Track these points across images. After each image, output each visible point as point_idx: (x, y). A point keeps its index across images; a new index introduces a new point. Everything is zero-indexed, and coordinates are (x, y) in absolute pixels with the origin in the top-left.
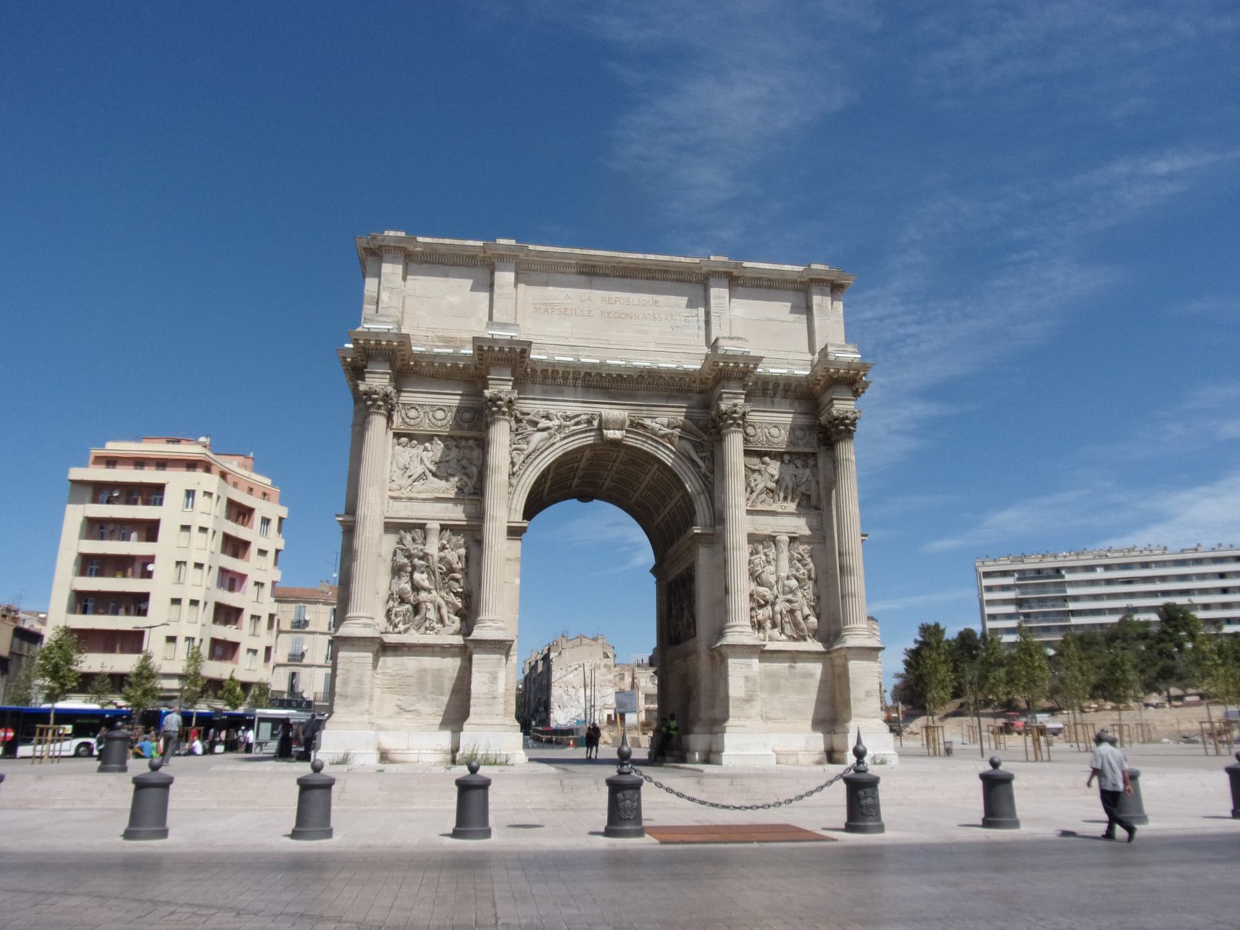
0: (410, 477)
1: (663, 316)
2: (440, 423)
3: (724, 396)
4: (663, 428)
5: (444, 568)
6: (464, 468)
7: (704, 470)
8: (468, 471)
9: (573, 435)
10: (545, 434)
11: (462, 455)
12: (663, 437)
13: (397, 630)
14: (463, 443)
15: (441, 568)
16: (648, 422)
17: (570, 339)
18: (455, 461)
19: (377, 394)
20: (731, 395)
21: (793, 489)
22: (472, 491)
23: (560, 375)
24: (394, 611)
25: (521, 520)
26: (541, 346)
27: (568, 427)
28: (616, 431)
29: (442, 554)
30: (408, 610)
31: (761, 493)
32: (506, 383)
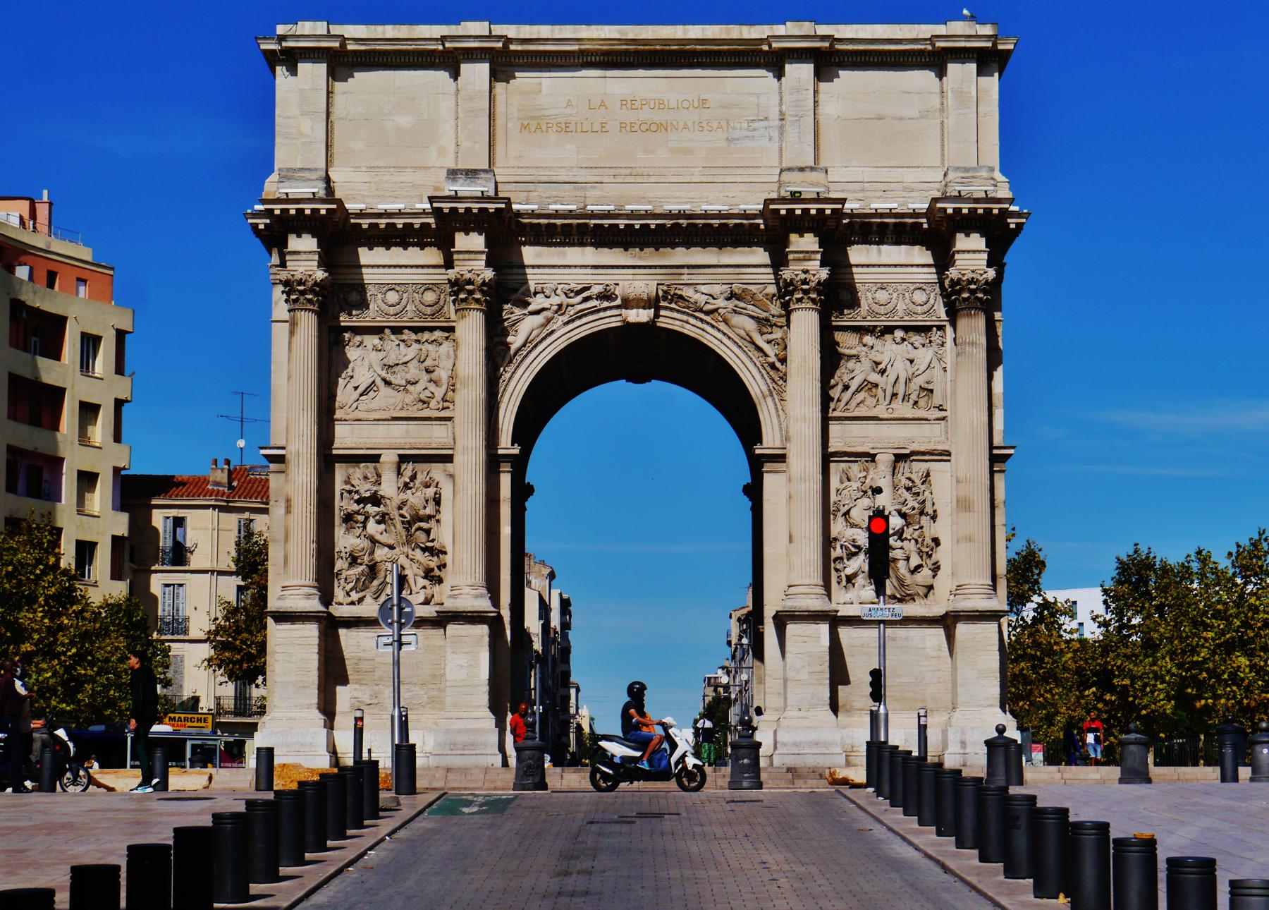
0: (356, 388)
1: (715, 124)
2: (392, 310)
3: (791, 257)
4: (711, 301)
5: (407, 515)
7: (772, 359)
8: (434, 376)
9: (580, 317)
10: (539, 319)
12: (708, 313)
13: (349, 600)
14: (426, 335)
15: (402, 516)
16: (688, 292)
17: (575, 170)
18: (415, 362)
19: (304, 285)
20: (801, 256)
21: (908, 381)
22: (441, 406)
23: (559, 230)
24: (343, 576)
25: (509, 446)
26: (531, 186)
27: (573, 306)
28: (641, 311)
29: (403, 496)
30: (362, 573)
31: (857, 391)
32: (479, 256)
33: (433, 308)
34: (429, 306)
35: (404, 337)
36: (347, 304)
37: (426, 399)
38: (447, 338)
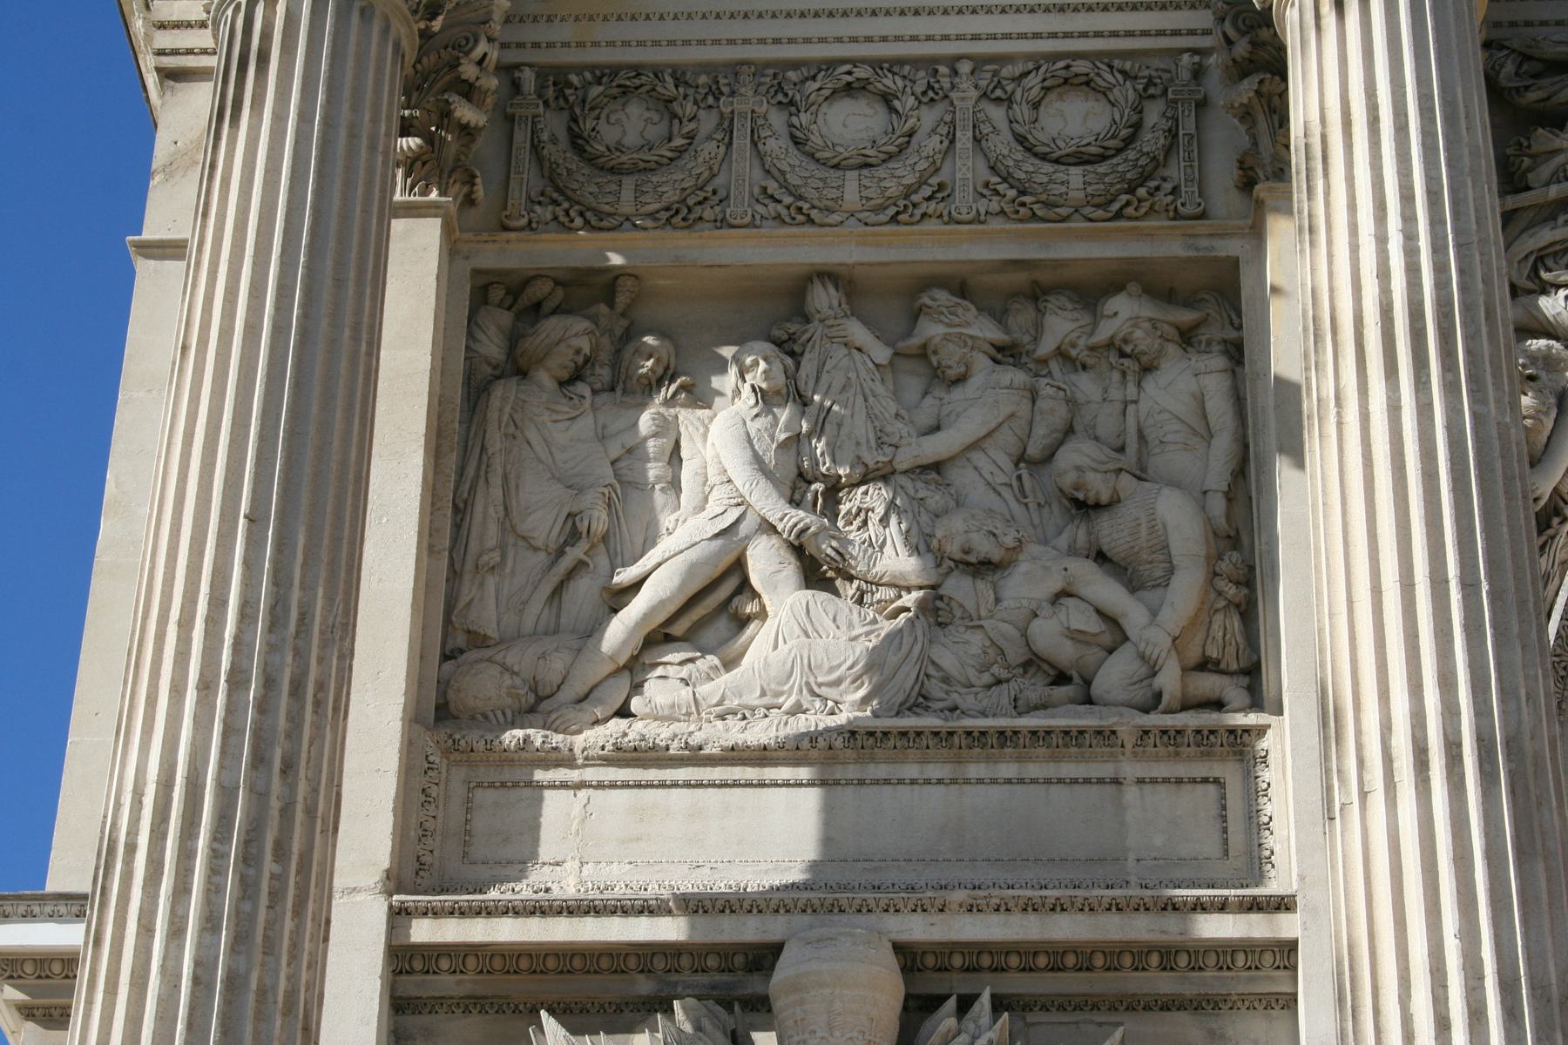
6: (1084, 508)
8: (1113, 532)
11: (1053, 412)
14: (1061, 325)
18: (996, 463)
33: (1102, 168)
34: (1080, 159)
35: (931, 330)
36: (591, 160)
37: (1067, 654)
38: (1187, 338)
